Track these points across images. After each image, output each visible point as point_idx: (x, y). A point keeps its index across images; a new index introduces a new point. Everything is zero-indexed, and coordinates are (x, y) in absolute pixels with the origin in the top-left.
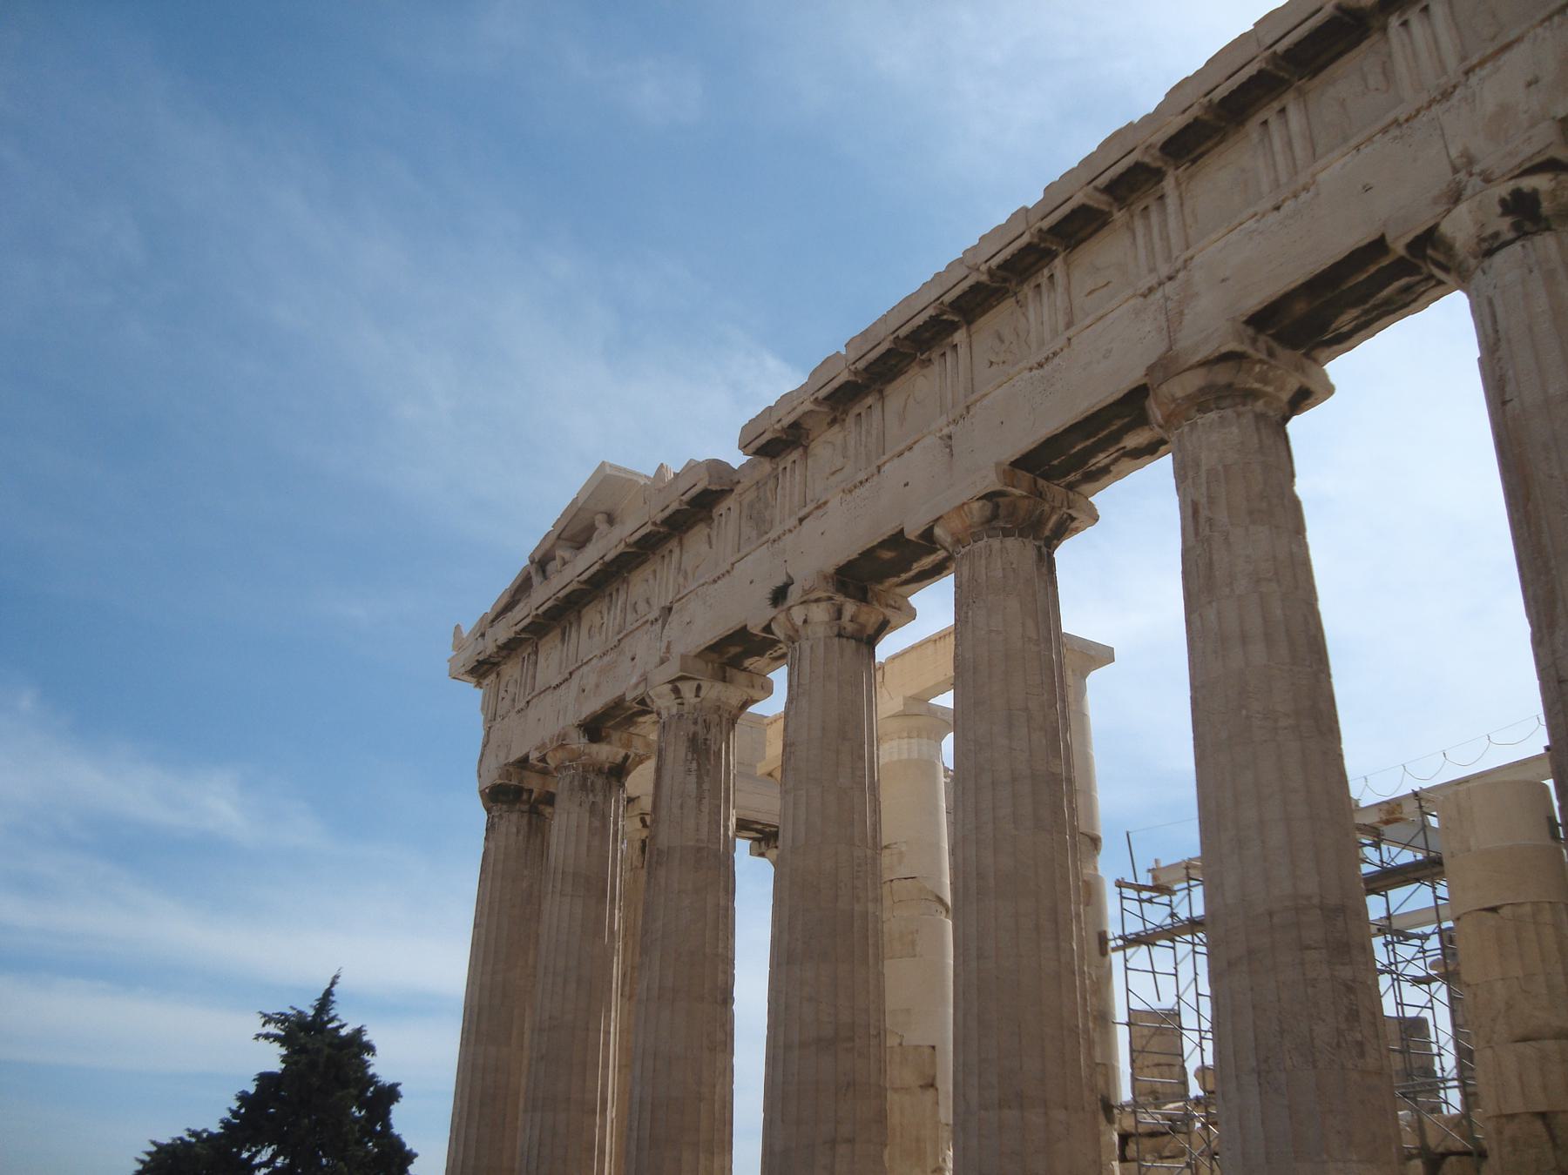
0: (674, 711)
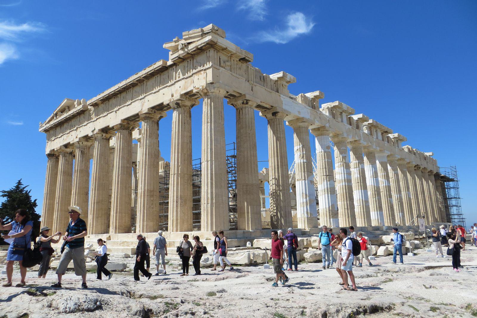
0: (78, 146)
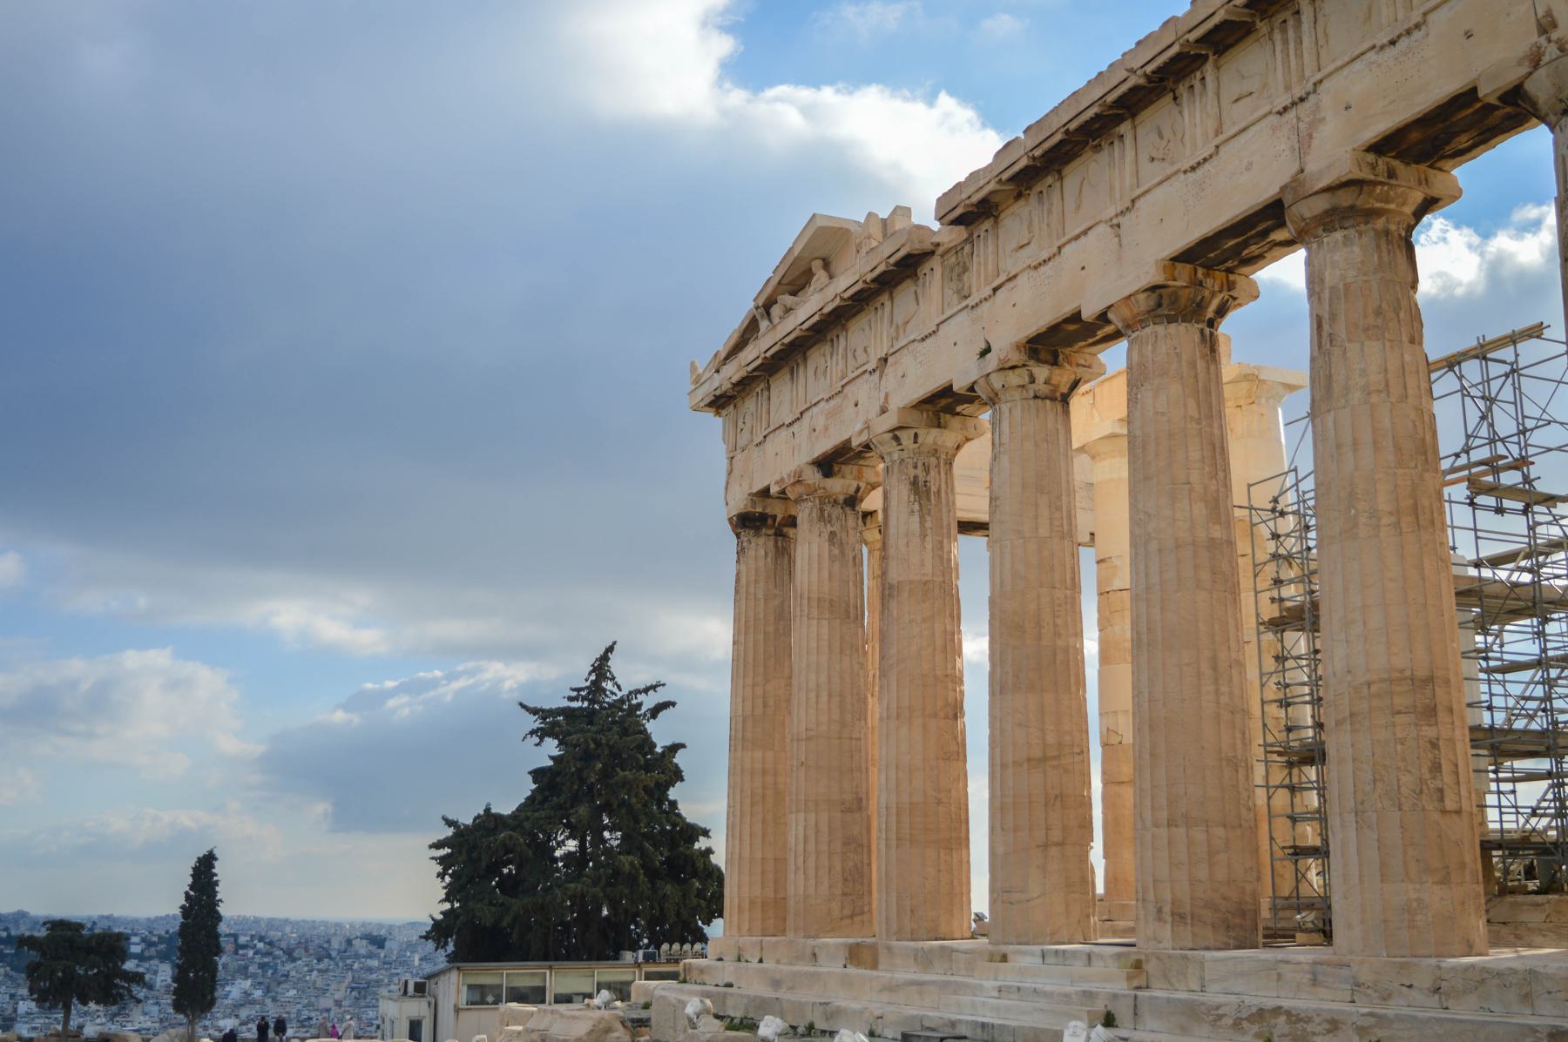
0: (896, 456)
